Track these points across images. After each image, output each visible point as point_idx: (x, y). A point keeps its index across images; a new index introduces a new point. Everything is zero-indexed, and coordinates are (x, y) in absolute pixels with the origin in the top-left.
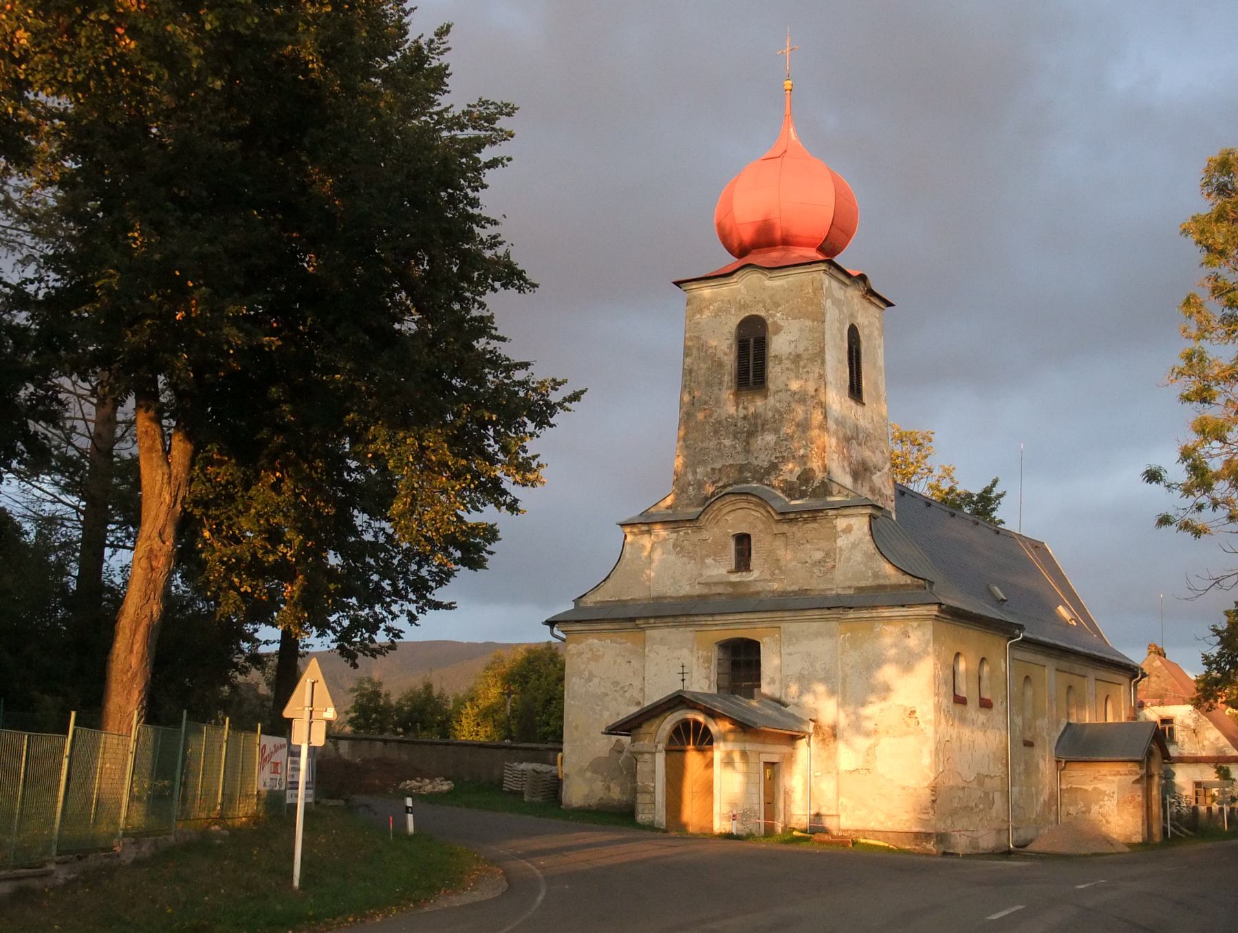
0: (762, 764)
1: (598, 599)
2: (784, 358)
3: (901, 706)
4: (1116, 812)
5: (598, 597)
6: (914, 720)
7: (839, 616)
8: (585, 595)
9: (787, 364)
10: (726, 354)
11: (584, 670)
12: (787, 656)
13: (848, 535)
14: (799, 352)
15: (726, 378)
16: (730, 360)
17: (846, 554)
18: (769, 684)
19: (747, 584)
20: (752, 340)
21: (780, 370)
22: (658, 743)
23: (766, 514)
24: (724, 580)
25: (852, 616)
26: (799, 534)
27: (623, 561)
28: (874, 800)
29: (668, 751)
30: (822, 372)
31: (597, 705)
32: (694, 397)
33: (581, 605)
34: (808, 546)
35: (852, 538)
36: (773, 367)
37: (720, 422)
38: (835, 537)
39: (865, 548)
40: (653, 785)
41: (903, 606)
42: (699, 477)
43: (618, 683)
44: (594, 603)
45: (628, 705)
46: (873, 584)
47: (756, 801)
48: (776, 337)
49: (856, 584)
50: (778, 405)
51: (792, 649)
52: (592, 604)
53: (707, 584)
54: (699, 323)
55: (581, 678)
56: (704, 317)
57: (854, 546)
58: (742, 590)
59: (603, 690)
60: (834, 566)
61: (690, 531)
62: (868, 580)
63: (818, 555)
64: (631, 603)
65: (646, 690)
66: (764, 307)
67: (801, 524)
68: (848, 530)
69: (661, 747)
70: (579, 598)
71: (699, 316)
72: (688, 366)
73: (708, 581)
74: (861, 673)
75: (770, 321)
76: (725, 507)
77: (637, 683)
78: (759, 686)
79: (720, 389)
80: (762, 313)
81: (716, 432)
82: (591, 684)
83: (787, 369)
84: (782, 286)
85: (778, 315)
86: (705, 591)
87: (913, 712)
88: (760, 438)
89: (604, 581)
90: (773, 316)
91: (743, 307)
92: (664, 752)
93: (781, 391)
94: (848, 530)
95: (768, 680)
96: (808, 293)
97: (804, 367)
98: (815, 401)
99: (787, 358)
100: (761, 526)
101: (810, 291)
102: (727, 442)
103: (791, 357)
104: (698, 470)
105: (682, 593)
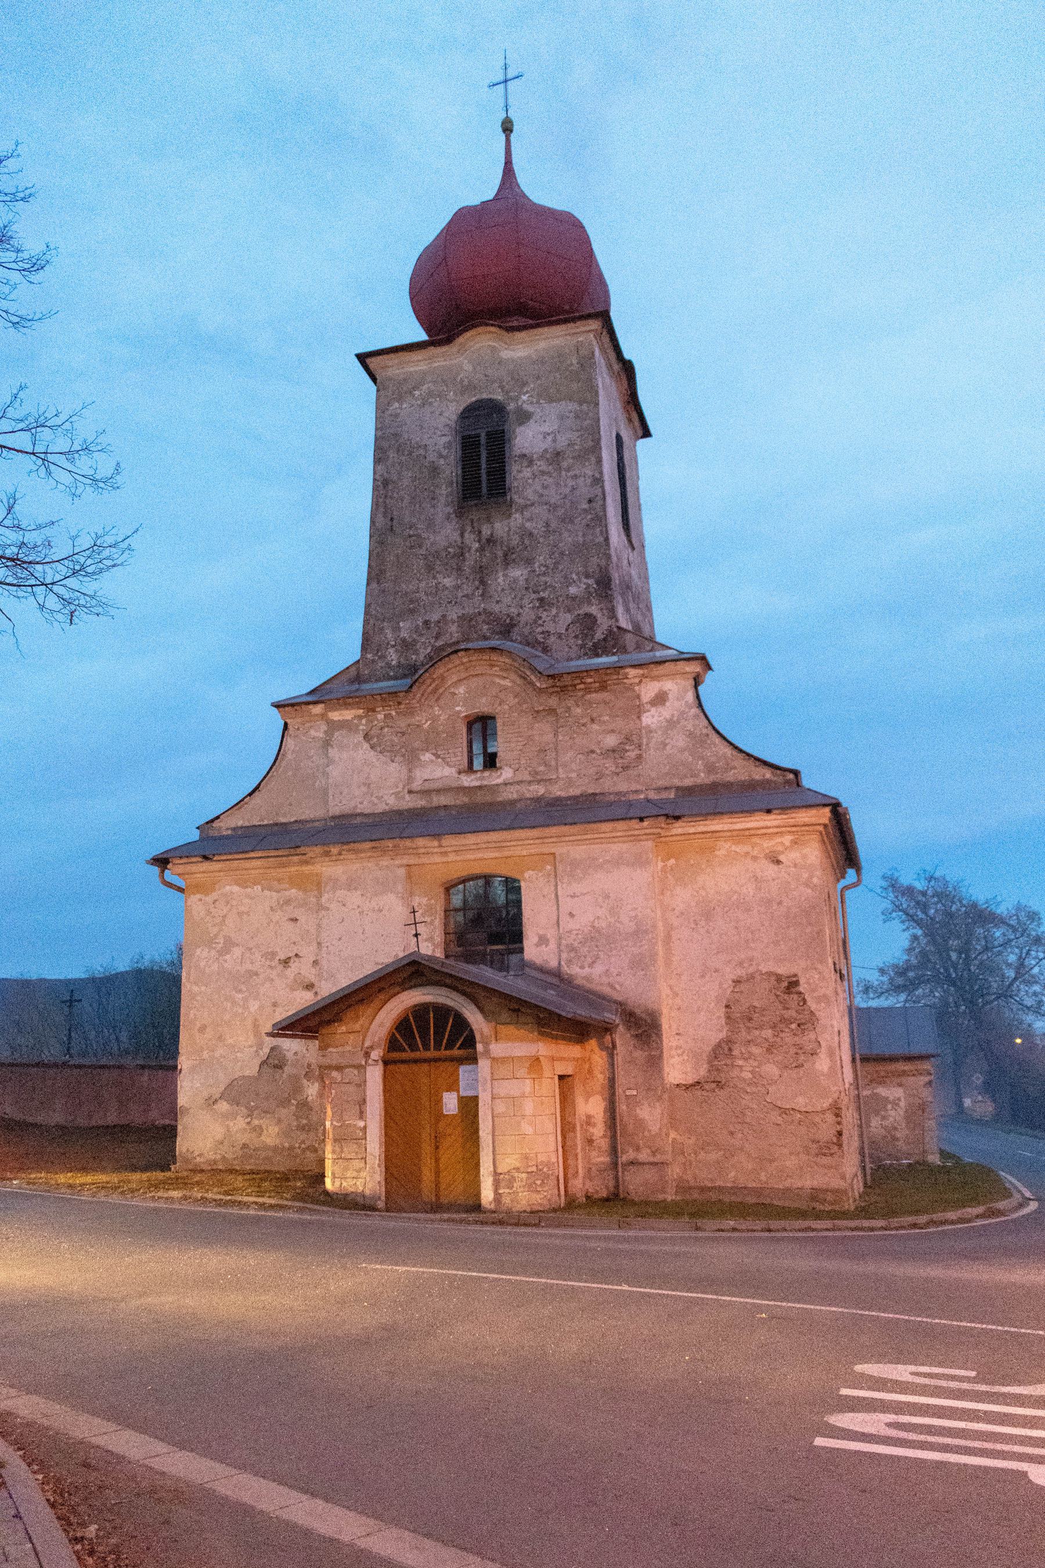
0: (556, 1078)
1: (240, 823)
2: (535, 456)
3: (770, 974)
4: (904, 1125)
5: (238, 820)
6: (795, 997)
7: (659, 830)
8: (218, 817)
9: (542, 465)
10: (441, 456)
11: (216, 936)
12: (569, 899)
13: (660, 709)
14: (559, 448)
15: (444, 490)
16: (450, 469)
17: (657, 737)
18: (537, 945)
19: (493, 789)
20: (483, 435)
21: (529, 475)
22: (372, 1047)
23: (519, 681)
24: (455, 784)
25: (680, 831)
26: (579, 710)
27: (283, 764)
28: (732, 1133)
29: (386, 1063)
30: (597, 475)
31: (240, 991)
32: (392, 519)
33: (211, 833)
34: (595, 727)
35: (666, 712)
36: (519, 472)
37: (437, 555)
38: (639, 711)
39: (690, 727)
40: (361, 1124)
41: (769, 811)
42: (404, 634)
43: (274, 954)
44: (234, 829)
45: (293, 990)
46: (707, 781)
47: (552, 1148)
48: (522, 428)
49: (677, 782)
50: (528, 525)
51: (577, 888)
52: (229, 832)
53: (426, 793)
54: (397, 416)
55: (211, 948)
56: (404, 406)
57: (671, 723)
58: (480, 798)
59: (249, 967)
60: (639, 757)
61: (394, 713)
62: (696, 776)
63: (611, 741)
64: (295, 827)
65: (324, 963)
66: (502, 387)
67: (580, 694)
68: (660, 699)
69: (376, 1054)
70: (207, 823)
71: (397, 405)
72: (382, 475)
73: (427, 786)
74: (696, 923)
75: (511, 407)
76: (451, 672)
77: (308, 952)
78: (521, 950)
79: (433, 506)
80: (499, 397)
81: (430, 568)
82: (228, 957)
83: (543, 473)
84: (529, 357)
85: (524, 398)
86: (421, 803)
87: (792, 985)
88: (501, 574)
89: (250, 794)
90: (517, 399)
91: (469, 387)
92: (380, 1063)
93: (532, 505)
94: (660, 699)
95: (535, 940)
96: (572, 364)
97: (568, 470)
98: (589, 517)
99: (542, 457)
100: (512, 701)
101: (575, 362)
102: (448, 582)
103: (548, 456)
104: (401, 624)
105: (381, 808)
